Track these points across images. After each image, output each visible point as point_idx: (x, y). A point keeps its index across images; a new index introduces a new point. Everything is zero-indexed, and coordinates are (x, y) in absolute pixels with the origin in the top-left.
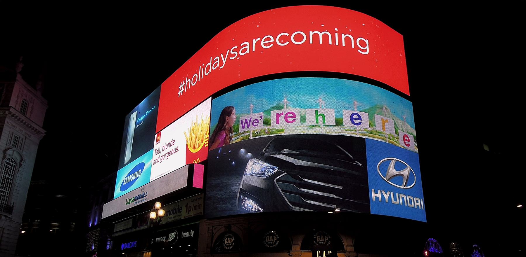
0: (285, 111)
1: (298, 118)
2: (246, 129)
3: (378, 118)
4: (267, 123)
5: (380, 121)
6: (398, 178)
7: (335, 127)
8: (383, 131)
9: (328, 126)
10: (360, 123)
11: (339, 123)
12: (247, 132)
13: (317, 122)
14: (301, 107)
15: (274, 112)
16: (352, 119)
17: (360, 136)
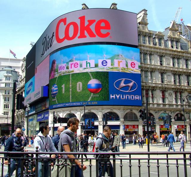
0: (74, 62)
1: (79, 66)
2: (60, 71)
3: (116, 61)
4: (67, 68)
5: (117, 62)
6: (126, 88)
7: (94, 68)
8: (118, 67)
9: (91, 68)
10: (106, 65)
11: (96, 66)
12: (61, 72)
13: (87, 67)
14: (80, 60)
15: (70, 63)
16: (102, 63)
17: (106, 71)
